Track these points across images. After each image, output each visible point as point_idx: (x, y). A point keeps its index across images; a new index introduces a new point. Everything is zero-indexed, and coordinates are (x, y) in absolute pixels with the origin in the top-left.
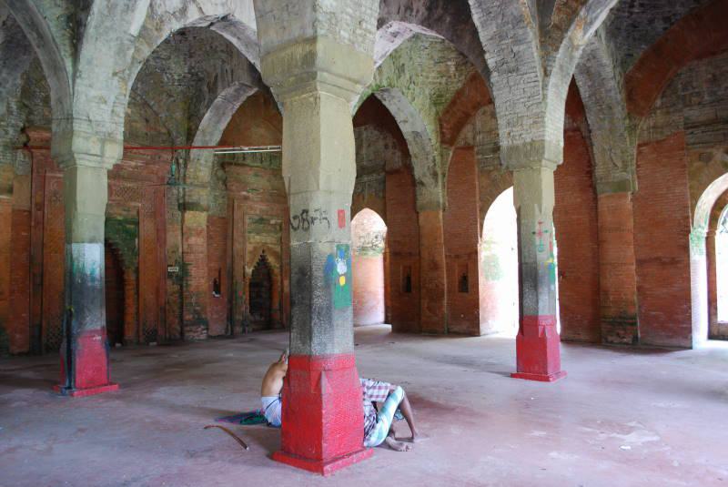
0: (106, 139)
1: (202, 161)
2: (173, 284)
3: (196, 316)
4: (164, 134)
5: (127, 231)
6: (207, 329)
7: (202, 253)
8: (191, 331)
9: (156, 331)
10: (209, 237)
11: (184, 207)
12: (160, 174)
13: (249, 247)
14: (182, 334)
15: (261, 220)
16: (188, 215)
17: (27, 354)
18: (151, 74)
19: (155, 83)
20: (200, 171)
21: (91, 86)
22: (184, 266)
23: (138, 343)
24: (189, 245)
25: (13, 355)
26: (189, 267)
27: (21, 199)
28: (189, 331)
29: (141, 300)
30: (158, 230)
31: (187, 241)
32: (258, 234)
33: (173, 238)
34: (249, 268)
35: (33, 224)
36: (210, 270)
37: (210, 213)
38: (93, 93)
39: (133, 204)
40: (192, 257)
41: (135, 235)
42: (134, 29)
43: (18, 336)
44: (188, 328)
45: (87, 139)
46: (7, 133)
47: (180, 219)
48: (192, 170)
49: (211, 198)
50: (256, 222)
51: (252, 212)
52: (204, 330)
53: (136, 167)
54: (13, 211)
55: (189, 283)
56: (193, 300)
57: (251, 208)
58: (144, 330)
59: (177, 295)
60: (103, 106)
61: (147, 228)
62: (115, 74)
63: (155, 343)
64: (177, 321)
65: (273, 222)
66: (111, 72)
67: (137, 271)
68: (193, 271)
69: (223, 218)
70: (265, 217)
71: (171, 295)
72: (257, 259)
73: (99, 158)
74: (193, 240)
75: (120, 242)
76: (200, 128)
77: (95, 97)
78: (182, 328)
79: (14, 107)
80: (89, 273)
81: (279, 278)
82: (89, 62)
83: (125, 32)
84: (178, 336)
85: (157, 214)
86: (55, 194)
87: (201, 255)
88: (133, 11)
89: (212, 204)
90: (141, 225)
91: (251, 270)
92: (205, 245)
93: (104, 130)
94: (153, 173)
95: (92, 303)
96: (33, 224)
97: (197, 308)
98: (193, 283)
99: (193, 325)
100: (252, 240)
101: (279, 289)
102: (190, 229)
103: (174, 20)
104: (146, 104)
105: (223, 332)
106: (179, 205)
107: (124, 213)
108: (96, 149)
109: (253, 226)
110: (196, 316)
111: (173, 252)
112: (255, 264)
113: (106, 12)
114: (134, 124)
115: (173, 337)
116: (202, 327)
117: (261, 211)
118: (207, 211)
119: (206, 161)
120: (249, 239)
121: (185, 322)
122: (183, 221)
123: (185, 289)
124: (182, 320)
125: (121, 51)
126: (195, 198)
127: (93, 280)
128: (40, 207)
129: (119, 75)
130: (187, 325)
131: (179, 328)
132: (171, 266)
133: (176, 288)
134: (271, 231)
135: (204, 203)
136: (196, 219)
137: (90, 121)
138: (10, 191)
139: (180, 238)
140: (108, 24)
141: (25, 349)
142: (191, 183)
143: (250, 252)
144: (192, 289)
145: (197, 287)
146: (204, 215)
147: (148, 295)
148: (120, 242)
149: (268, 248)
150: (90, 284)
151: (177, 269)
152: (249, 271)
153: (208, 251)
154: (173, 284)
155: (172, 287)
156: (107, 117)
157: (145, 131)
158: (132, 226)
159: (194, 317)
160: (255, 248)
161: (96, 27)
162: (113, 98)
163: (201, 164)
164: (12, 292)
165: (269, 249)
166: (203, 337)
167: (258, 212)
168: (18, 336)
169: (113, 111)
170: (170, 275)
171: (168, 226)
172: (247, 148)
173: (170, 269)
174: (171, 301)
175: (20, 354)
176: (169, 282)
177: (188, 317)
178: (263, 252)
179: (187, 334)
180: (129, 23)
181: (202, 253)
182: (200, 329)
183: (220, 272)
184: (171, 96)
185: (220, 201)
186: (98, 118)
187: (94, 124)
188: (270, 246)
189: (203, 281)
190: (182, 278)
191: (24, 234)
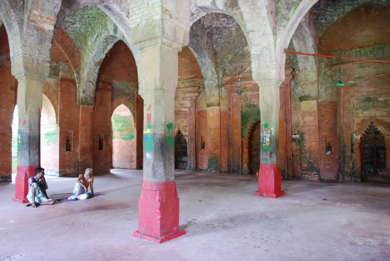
1: (309, 69)
3: (310, 165)
8: (307, 174)
9: (285, 170)
11: (302, 99)
13: (357, 120)
15: (368, 99)
16: (304, 104)
22: (302, 134)
24: (304, 122)
26: (304, 135)
27: (224, 108)
28: (305, 174)
34: (358, 135)
40: (306, 128)
43: (224, 164)
44: (305, 172)
48: (303, 76)
50: (364, 101)
51: (360, 95)
52: (316, 174)
54: (221, 112)
55: (305, 144)
56: (307, 155)
57: (358, 92)
59: (299, 152)
64: (299, 167)
65: (381, 99)
68: (307, 137)
69: (332, 102)
86: (236, 102)
87: (313, 128)
91: (359, 137)
92: (317, 120)
97: (311, 160)
98: (307, 145)
99: (308, 170)
105: (334, 178)
109: (362, 105)
110: (310, 165)
111: (296, 126)
112: (363, 132)
116: (315, 173)
120: (358, 114)
126: (307, 93)
132: (296, 134)
134: (380, 107)
135: (314, 94)
136: (311, 106)
138: (219, 104)
141: (227, 170)
142: (304, 84)
143: (358, 124)
144: (306, 148)
145: (310, 147)
146: (315, 101)
151: (297, 136)
152: (357, 137)
159: (308, 165)
160: (363, 121)
161: (134, 50)
163: (308, 71)
164: (221, 146)
165: (378, 121)
170: (294, 140)
173: (294, 136)
174: (295, 155)
175: (225, 172)
176: (294, 144)
177: (305, 165)
182: (312, 174)
185: (330, 91)
188: (379, 118)
189: (314, 144)
190: (300, 142)
191: (225, 122)
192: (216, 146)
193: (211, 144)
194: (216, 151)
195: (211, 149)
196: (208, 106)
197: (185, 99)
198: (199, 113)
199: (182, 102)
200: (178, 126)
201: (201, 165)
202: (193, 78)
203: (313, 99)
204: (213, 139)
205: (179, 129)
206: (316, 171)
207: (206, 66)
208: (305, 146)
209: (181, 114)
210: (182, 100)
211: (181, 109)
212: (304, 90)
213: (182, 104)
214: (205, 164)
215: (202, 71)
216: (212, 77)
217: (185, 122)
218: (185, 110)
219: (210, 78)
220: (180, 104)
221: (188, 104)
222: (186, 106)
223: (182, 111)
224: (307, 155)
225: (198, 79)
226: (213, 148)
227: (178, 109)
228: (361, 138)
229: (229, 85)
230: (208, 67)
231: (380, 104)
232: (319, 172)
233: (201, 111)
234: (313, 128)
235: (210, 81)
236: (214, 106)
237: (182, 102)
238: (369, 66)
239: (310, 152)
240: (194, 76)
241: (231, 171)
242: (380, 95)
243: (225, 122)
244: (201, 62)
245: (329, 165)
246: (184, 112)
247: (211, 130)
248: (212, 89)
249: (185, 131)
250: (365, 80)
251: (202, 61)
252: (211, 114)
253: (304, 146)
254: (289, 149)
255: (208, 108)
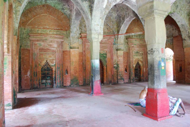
0: (99, 34)
1: (121, 38)
2: (115, 69)
3: (121, 78)
4: (112, 32)
5: (104, 56)
6: (124, 81)
7: (122, 61)
10: (124, 57)
11: (117, 50)
12: (111, 42)
13: (134, 60)
14: (117, 82)
15: (137, 52)
16: (118, 52)
17: (83, 85)
18: (108, 17)
19: (109, 19)
20: (121, 40)
21: (95, 22)
22: (118, 65)
23: (107, 84)
25: (80, 85)
26: (119, 65)
27: (80, 50)
29: (107, 73)
30: (111, 56)
31: (118, 58)
32: (136, 56)
33: (115, 58)
35: (83, 55)
36: (124, 66)
37: (124, 51)
38: (96, 23)
39: (105, 50)
40: (120, 62)
41: (106, 57)
42: (104, 6)
43: (81, 81)
44: (119, 81)
45: (95, 34)
46: (77, 35)
47: (116, 53)
49: (124, 47)
51: (135, 50)
52: (123, 81)
53: (106, 41)
54: (79, 53)
55: (119, 69)
56: (120, 73)
58: (108, 81)
60: (98, 26)
61: (109, 56)
62: (100, 18)
63: (111, 84)
64: (116, 79)
65: (140, 53)
66: (99, 18)
67: (107, 66)
68: (120, 66)
69: (128, 52)
70: (138, 51)
71: (115, 72)
72: (136, 63)
73: (98, 39)
74: (120, 58)
75: (102, 59)
76: (121, 29)
77: (96, 24)
78: (117, 81)
79: (78, 29)
80: (96, 66)
81: (142, 68)
82: (95, 16)
83: (102, 7)
84: (117, 82)
85: (111, 52)
87: (122, 62)
88: (104, 2)
89: (124, 49)
90: (107, 55)
91: (135, 65)
92: (123, 59)
93: (99, 32)
94: (109, 42)
95: (97, 74)
96: (83, 55)
97: (121, 75)
98: (120, 69)
100: (135, 58)
101: (142, 71)
102: (119, 55)
103: (113, 3)
104: (107, 25)
105: (128, 82)
106: (116, 49)
107: (103, 52)
108: (97, 37)
109: (135, 54)
111: (115, 61)
112: (136, 64)
113: (98, 3)
114: (105, 30)
115: (115, 83)
116: (123, 80)
117: (137, 50)
118: (123, 50)
119: (122, 38)
120: (134, 57)
121: (118, 79)
122: (117, 53)
123: (118, 71)
124: (117, 78)
125: (101, 13)
126: (120, 48)
127: (97, 68)
128: (85, 51)
129: (101, 18)
130: (119, 80)
131: (117, 81)
133: (116, 70)
135: (122, 49)
136: (121, 53)
137: (95, 30)
138: (78, 48)
139: (116, 57)
140: (98, 6)
141: (82, 85)
142: (119, 44)
143: (135, 61)
144: (120, 71)
145: (121, 70)
147: (109, 72)
148: (102, 59)
149: (140, 60)
150: (96, 69)
151: (116, 66)
152: (134, 66)
153: (124, 61)
154: (115, 69)
155: (115, 70)
156: (99, 29)
157: (107, 32)
158: (105, 55)
160: (136, 60)
161: (95, 7)
162: (100, 24)
163: (121, 39)
164: (79, 71)
166: (123, 83)
167: (136, 50)
168: (81, 81)
169: (100, 27)
170: (114, 67)
171: (114, 55)
172: (133, 34)
173: (114, 66)
175: (81, 85)
176: (114, 69)
177: (119, 78)
178: (138, 61)
179: (119, 82)
180: (103, 5)
181: (122, 61)
183: (127, 66)
184: (113, 22)
185: (127, 48)
186: (97, 29)
187: (96, 31)
188: (140, 59)
189: (122, 69)
190: (117, 68)
191: (81, 58)
192: (77, 72)
193: (73, 71)
194: (76, 75)
195: (73, 73)
196: (71, 48)
197: (52, 42)
198: (64, 52)
199: (51, 43)
200: (46, 59)
201: (65, 84)
202: (59, 29)
203: (122, 50)
204: (75, 68)
205: (47, 61)
206: (123, 79)
207: (75, 25)
208: (120, 70)
209: (49, 51)
210: (51, 42)
211: (50, 48)
212: (119, 46)
213: (51, 45)
214: (68, 83)
215: (71, 27)
216: (76, 32)
217: (52, 57)
218: (53, 49)
219: (74, 33)
220: (49, 45)
221: (55, 45)
222: (54, 46)
223: (50, 50)
224: (120, 73)
225: (62, 31)
226: (75, 73)
227: (48, 48)
228: (135, 66)
229: (85, 38)
230: (76, 26)
231: (139, 54)
232: (124, 80)
233: (66, 51)
234: (122, 62)
235: (74, 34)
236: (75, 48)
237: (51, 43)
238: (137, 41)
239: (121, 72)
240: (60, 28)
241: (86, 84)
242: (140, 51)
243: (81, 58)
244: (74, 22)
245: (126, 77)
246: (52, 50)
247: (73, 62)
248: (74, 39)
249: (53, 63)
250: (136, 45)
251: (74, 22)
252: (73, 53)
253: (119, 70)
254: (112, 71)
255: (71, 49)
